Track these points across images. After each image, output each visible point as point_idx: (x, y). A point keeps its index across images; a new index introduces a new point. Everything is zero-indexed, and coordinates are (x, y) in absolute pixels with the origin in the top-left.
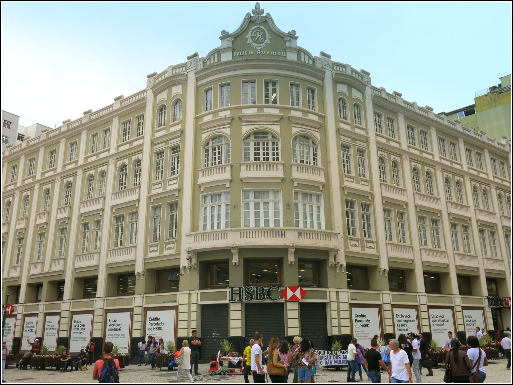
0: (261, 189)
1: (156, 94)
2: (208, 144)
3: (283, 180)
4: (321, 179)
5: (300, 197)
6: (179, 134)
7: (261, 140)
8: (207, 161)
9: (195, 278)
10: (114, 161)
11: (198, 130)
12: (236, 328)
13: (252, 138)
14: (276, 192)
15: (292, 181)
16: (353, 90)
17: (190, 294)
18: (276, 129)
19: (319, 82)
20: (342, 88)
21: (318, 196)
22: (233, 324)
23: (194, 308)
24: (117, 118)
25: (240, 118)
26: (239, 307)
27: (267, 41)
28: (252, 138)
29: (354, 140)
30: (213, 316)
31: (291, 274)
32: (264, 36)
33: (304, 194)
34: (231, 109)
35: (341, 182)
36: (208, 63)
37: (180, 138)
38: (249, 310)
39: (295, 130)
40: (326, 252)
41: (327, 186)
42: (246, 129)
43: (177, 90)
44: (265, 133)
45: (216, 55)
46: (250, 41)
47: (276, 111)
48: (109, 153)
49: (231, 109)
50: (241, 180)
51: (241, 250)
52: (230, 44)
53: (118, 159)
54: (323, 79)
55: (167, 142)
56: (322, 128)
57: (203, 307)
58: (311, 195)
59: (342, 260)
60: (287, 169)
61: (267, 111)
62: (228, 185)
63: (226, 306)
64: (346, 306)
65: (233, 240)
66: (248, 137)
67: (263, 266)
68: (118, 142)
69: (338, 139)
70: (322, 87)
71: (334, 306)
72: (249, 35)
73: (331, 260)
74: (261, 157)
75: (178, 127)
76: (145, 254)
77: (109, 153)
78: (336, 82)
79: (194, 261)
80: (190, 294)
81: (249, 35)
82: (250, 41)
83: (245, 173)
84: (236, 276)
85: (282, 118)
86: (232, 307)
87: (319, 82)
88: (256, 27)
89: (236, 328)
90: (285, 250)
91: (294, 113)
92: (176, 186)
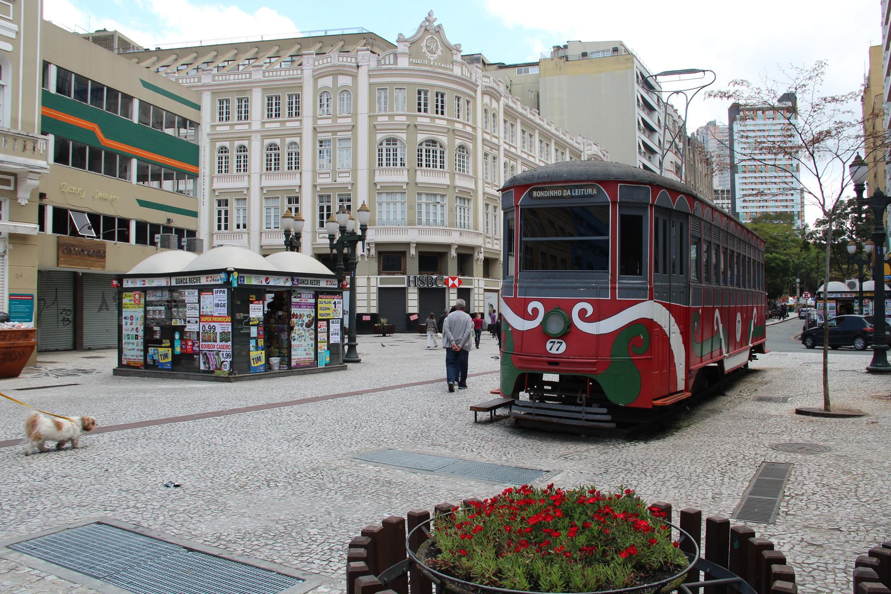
0: (433, 193)
1: (316, 78)
2: (381, 144)
3: (448, 186)
4: (473, 187)
5: (458, 200)
6: (350, 128)
7: (431, 148)
8: (380, 160)
9: (375, 265)
10: (259, 137)
11: (373, 129)
12: (413, 305)
13: (424, 145)
14: (443, 196)
15: (455, 187)
16: (493, 100)
17: (369, 279)
18: (444, 139)
19: (473, 94)
20: (487, 99)
21: (469, 200)
22: (410, 303)
23: (374, 290)
25: (415, 126)
27: (439, 52)
29: (492, 148)
30: (391, 298)
31: (452, 265)
32: (437, 48)
33: (460, 198)
34: (407, 116)
35: (484, 189)
37: (350, 133)
38: (422, 292)
39: (458, 142)
40: (472, 248)
41: (475, 191)
42: (421, 137)
43: (344, 81)
44: (434, 142)
46: (424, 50)
47: (444, 123)
49: (407, 116)
50: (416, 184)
51: (418, 245)
52: (406, 50)
53: (264, 137)
54: (475, 92)
55: (334, 133)
56: (473, 138)
57: (380, 288)
58: (464, 199)
59: (482, 256)
60: (453, 176)
61: (439, 122)
62: (405, 187)
63: (403, 291)
64: (482, 291)
65: (412, 236)
66: (421, 144)
67: (432, 259)
68: (263, 118)
69: (483, 148)
70: (475, 99)
71: (476, 291)
72: (424, 43)
73: (476, 254)
74: (431, 163)
75: (349, 121)
76: (314, 239)
78: (484, 93)
79: (373, 251)
80: (369, 279)
81: (424, 43)
82: (424, 50)
83: (422, 178)
84: (412, 265)
85: (449, 129)
87: (473, 94)
89: (413, 305)
90: (449, 246)
91: (458, 126)
92: (349, 180)
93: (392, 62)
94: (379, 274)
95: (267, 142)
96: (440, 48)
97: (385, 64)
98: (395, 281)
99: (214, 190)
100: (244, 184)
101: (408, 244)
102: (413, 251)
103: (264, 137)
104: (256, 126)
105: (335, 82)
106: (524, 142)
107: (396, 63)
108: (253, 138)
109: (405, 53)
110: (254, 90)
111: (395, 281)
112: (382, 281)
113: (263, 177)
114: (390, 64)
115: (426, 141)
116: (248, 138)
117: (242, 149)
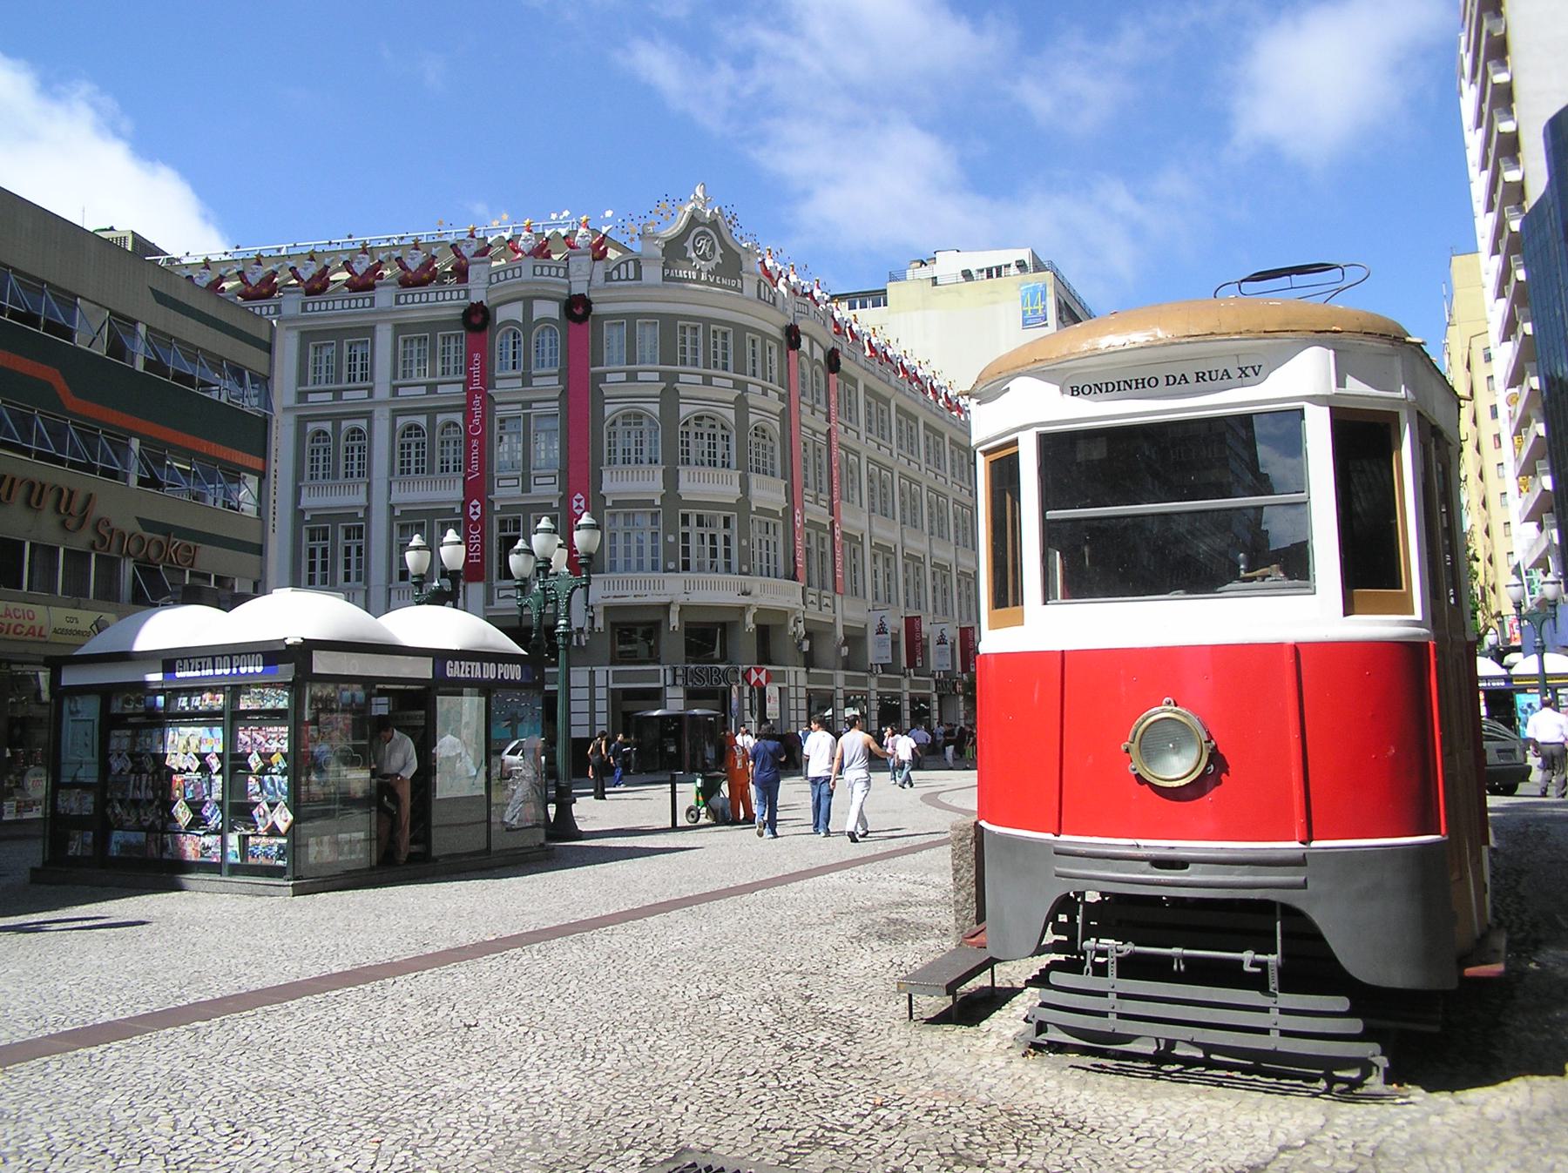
10: (387, 414)
17: (592, 673)
23: (601, 693)
24: (389, 326)
26: (680, 692)
28: (692, 423)
36: (615, 276)
40: (784, 614)
45: (631, 264)
48: (370, 396)
51: (683, 608)
67: (707, 635)
68: (395, 377)
71: (792, 690)
77: (370, 396)
79: (600, 623)
80: (592, 673)
86: (670, 692)
88: (700, 229)
93: (632, 276)
94: (613, 663)
95: (402, 421)
96: (719, 251)
97: (619, 279)
98: (639, 676)
99: (303, 512)
100: (361, 499)
101: (666, 607)
102: (674, 620)
103: (396, 413)
104: (382, 391)
105: (528, 311)
106: (870, 422)
107: (638, 276)
108: (376, 415)
109: (657, 259)
110: (378, 327)
111: (639, 676)
112: (618, 677)
113: (395, 487)
114: (627, 279)
115: (696, 418)
116: (368, 416)
117: (355, 433)
